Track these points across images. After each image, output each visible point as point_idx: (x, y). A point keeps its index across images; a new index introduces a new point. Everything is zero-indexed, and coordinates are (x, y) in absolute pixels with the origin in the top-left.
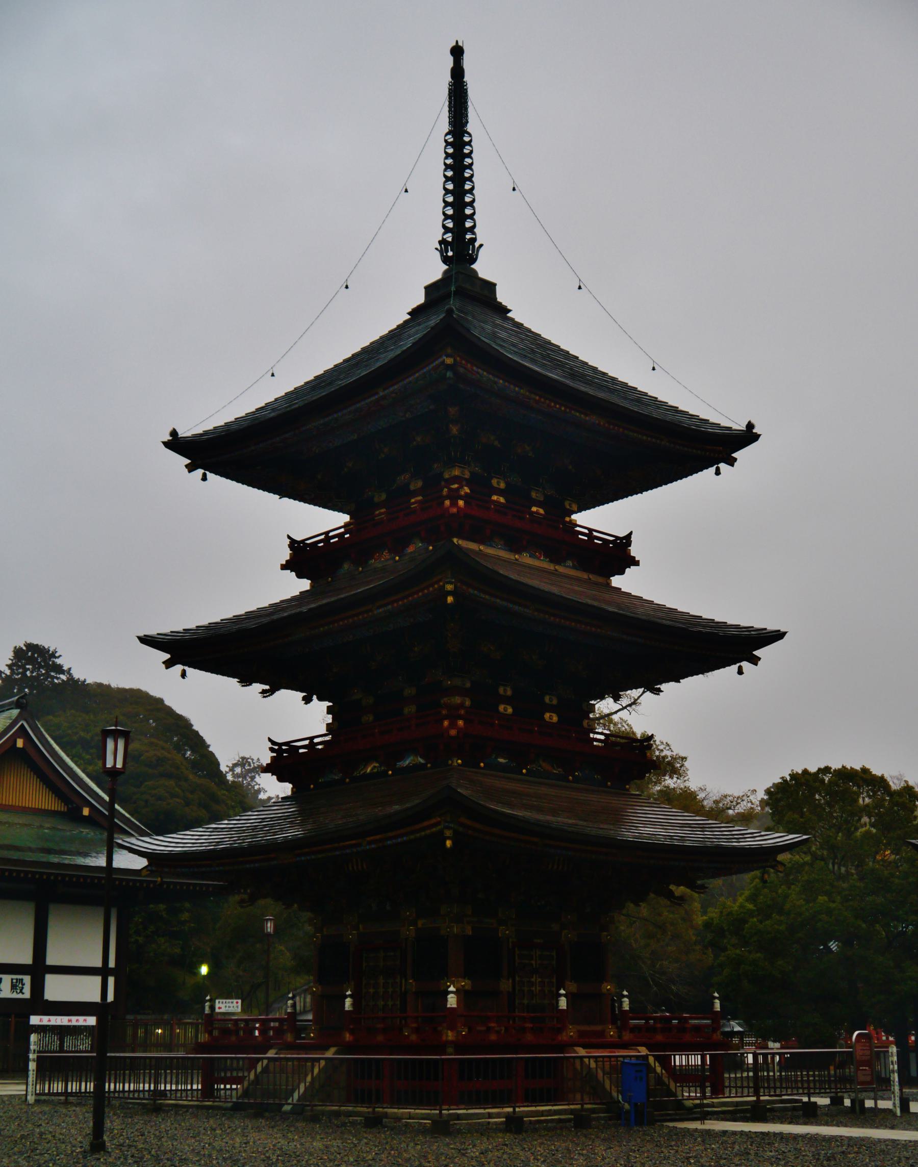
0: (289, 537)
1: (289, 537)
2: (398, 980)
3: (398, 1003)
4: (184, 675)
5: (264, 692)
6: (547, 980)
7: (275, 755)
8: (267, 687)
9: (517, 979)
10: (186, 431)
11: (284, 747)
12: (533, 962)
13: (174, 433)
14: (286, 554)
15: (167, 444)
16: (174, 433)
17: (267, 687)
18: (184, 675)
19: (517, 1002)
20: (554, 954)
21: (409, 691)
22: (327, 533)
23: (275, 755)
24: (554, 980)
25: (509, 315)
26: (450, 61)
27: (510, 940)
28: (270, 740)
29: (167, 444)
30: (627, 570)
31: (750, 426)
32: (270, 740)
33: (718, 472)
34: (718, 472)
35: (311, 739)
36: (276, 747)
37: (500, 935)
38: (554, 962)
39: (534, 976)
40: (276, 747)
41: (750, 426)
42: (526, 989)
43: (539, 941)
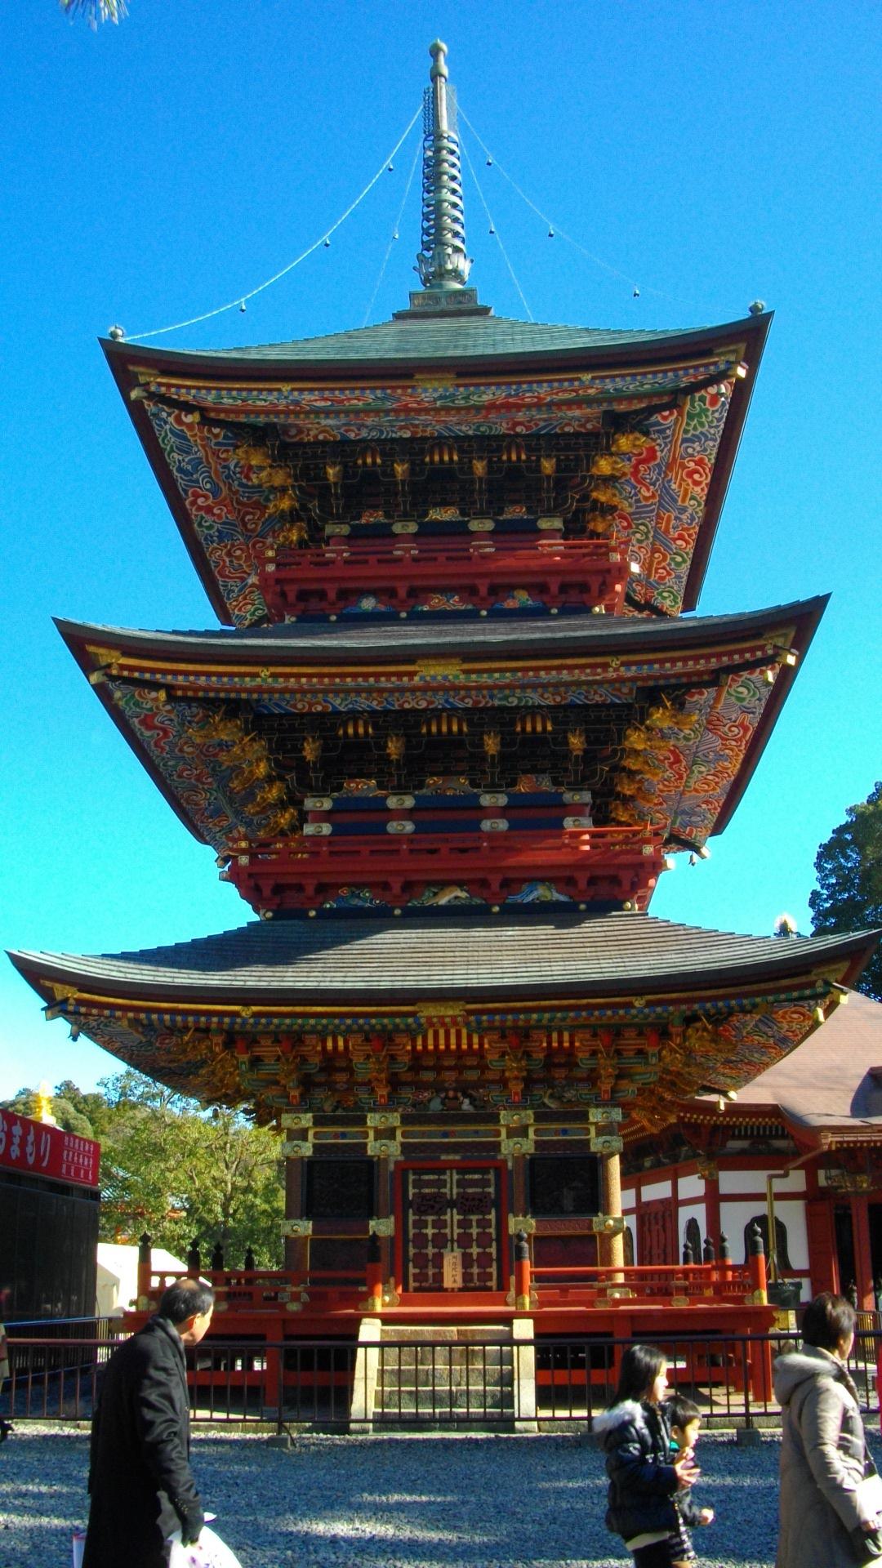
9: (411, 1218)
12: (446, 1190)
19: (412, 1251)
20: (491, 1176)
24: (492, 1216)
27: (392, 1159)
31: (754, 309)
38: (491, 1190)
39: (449, 1210)
42: (430, 1231)
43: (451, 1157)
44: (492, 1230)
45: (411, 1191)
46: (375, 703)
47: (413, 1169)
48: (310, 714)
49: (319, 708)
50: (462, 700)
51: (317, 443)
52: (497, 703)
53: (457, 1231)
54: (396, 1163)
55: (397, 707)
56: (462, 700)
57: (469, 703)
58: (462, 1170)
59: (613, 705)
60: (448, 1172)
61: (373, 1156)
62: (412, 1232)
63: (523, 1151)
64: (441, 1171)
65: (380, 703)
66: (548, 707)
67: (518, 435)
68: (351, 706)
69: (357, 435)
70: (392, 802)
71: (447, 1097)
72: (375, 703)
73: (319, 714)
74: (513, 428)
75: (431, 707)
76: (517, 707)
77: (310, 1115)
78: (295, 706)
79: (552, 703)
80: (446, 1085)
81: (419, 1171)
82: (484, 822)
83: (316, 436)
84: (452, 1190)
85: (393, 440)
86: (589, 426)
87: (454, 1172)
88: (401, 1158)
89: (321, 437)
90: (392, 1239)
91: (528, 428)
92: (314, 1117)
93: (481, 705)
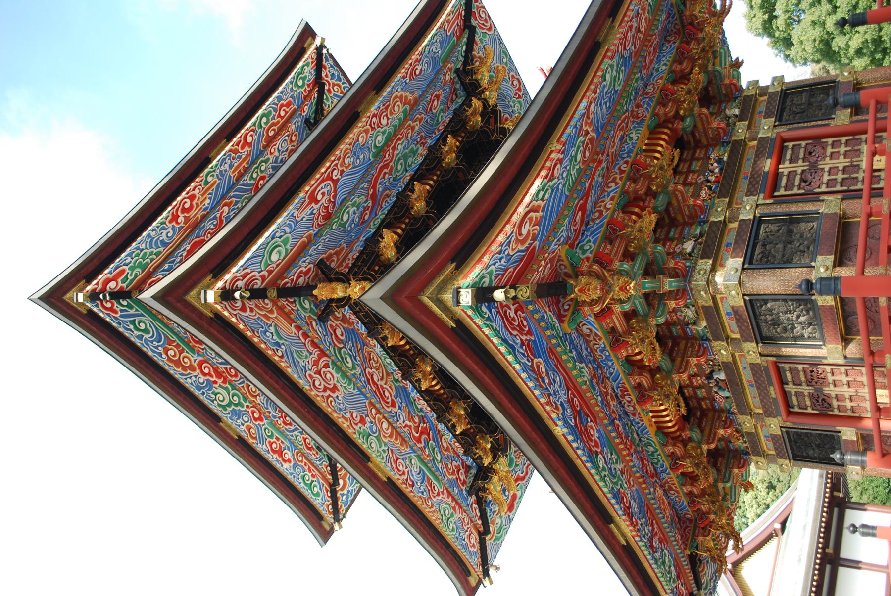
2: (828, 368)
6: (829, 150)
9: (823, 189)
12: (799, 170)
20: (790, 145)
24: (830, 140)
27: (760, 202)
38: (803, 143)
42: (840, 176)
44: (844, 139)
45: (796, 191)
47: (775, 191)
53: (842, 159)
54: (764, 199)
58: (780, 161)
60: (780, 170)
62: (838, 188)
63: (772, 124)
64: (777, 176)
80: (700, 181)
81: (775, 186)
84: (800, 166)
87: (780, 166)
88: (762, 196)
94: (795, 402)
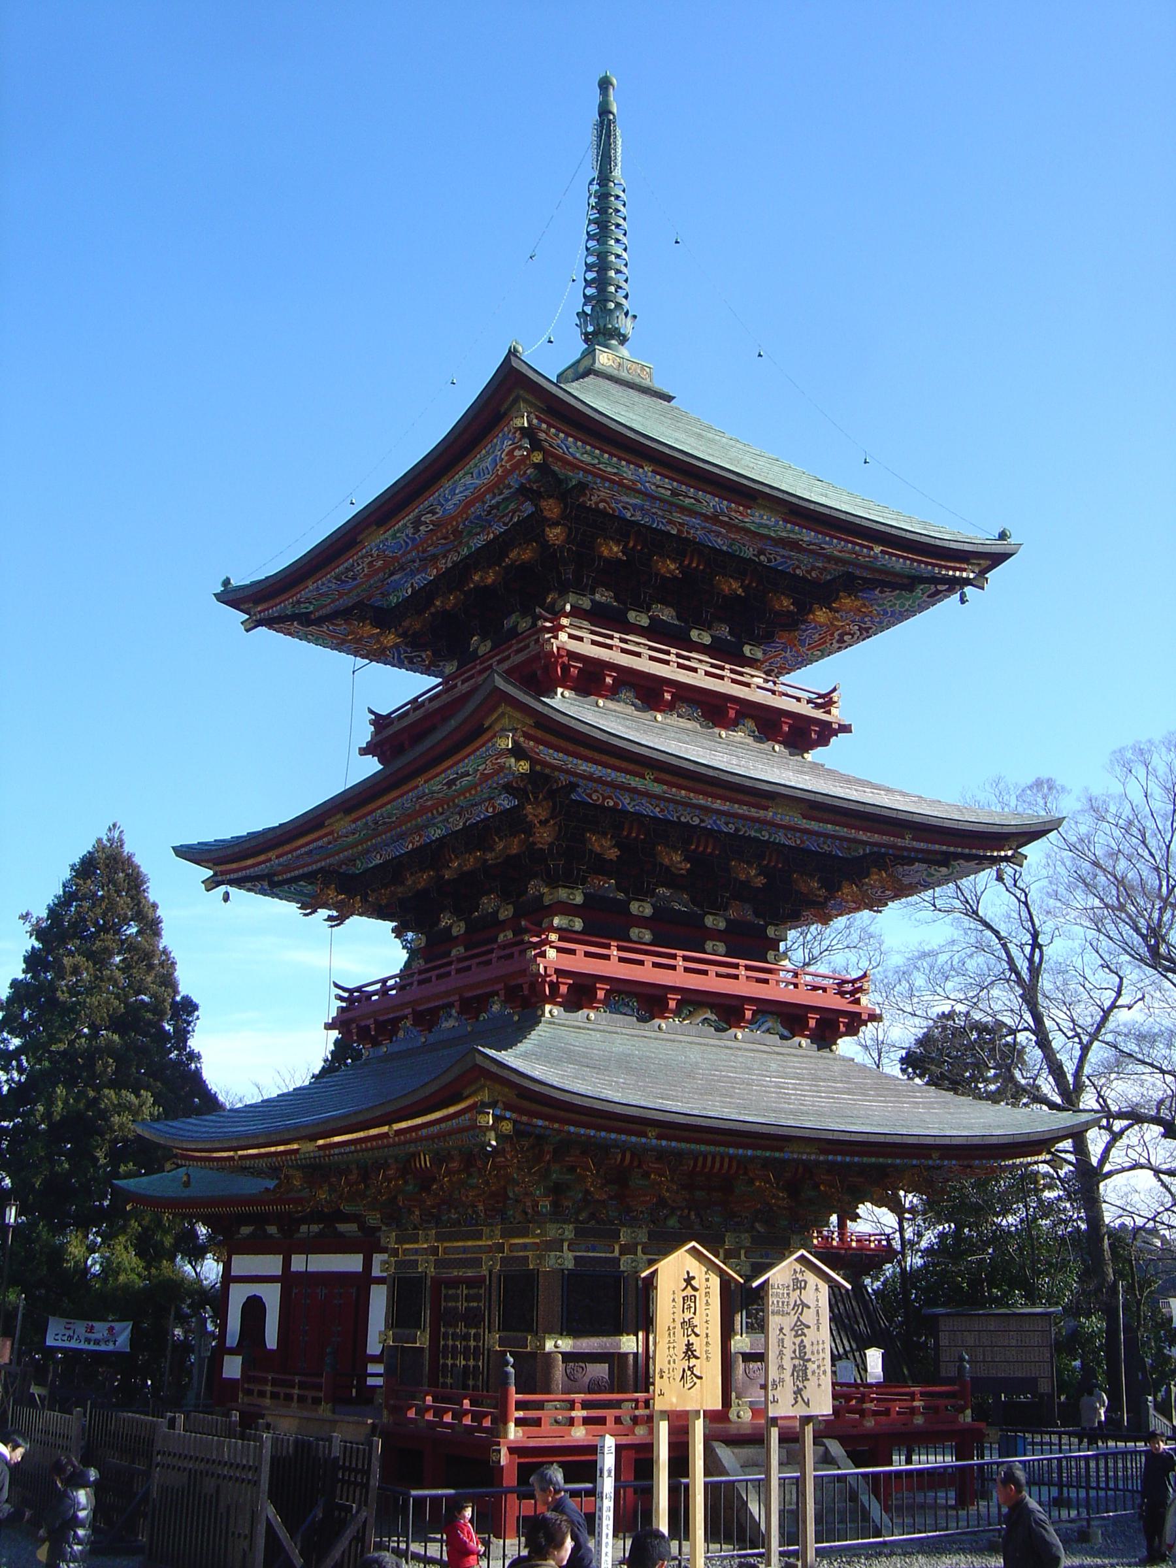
0: (371, 712)
1: (371, 712)
3: (480, 1364)
4: (226, 898)
5: (330, 918)
7: (344, 1004)
8: (335, 913)
10: (242, 578)
11: (356, 994)
13: (226, 582)
14: (366, 733)
15: (219, 597)
16: (226, 582)
17: (335, 913)
18: (226, 898)
21: (506, 913)
22: (416, 699)
23: (344, 1004)
25: (673, 403)
26: (596, 98)
28: (337, 986)
29: (219, 597)
30: (833, 739)
32: (337, 986)
33: (963, 600)
34: (963, 600)
35: (384, 981)
36: (346, 995)
37: (622, 1268)
40: (346, 995)
41: (1003, 536)
46: (658, 809)
48: (602, 807)
49: (611, 804)
50: (727, 824)
51: (597, 511)
52: (753, 834)
55: (675, 819)
56: (727, 824)
57: (731, 829)
59: (837, 856)
61: (624, 1272)
65: (662, 810)
66: (790, 847)
67: (760, 563)
68: (637, 808)
69: (632, 515)
70: (634, 907)
71: (681, 1216)
72: (658, 809)
73: (609, 808)
74: (758, 556)
75: (703, 825)
76: (767, 842)
77: (571, 1227)
78: (590, 796)
79: (794, 844)
82: (708, 942)
83: (597, 504)
85: (661, 531)
86: (814, 574)
89: (602, 505)
90: (636, 1355)
91: (769, 561)
92: (575, 1228)
93: (741, 833)
94: (450, 1292)
